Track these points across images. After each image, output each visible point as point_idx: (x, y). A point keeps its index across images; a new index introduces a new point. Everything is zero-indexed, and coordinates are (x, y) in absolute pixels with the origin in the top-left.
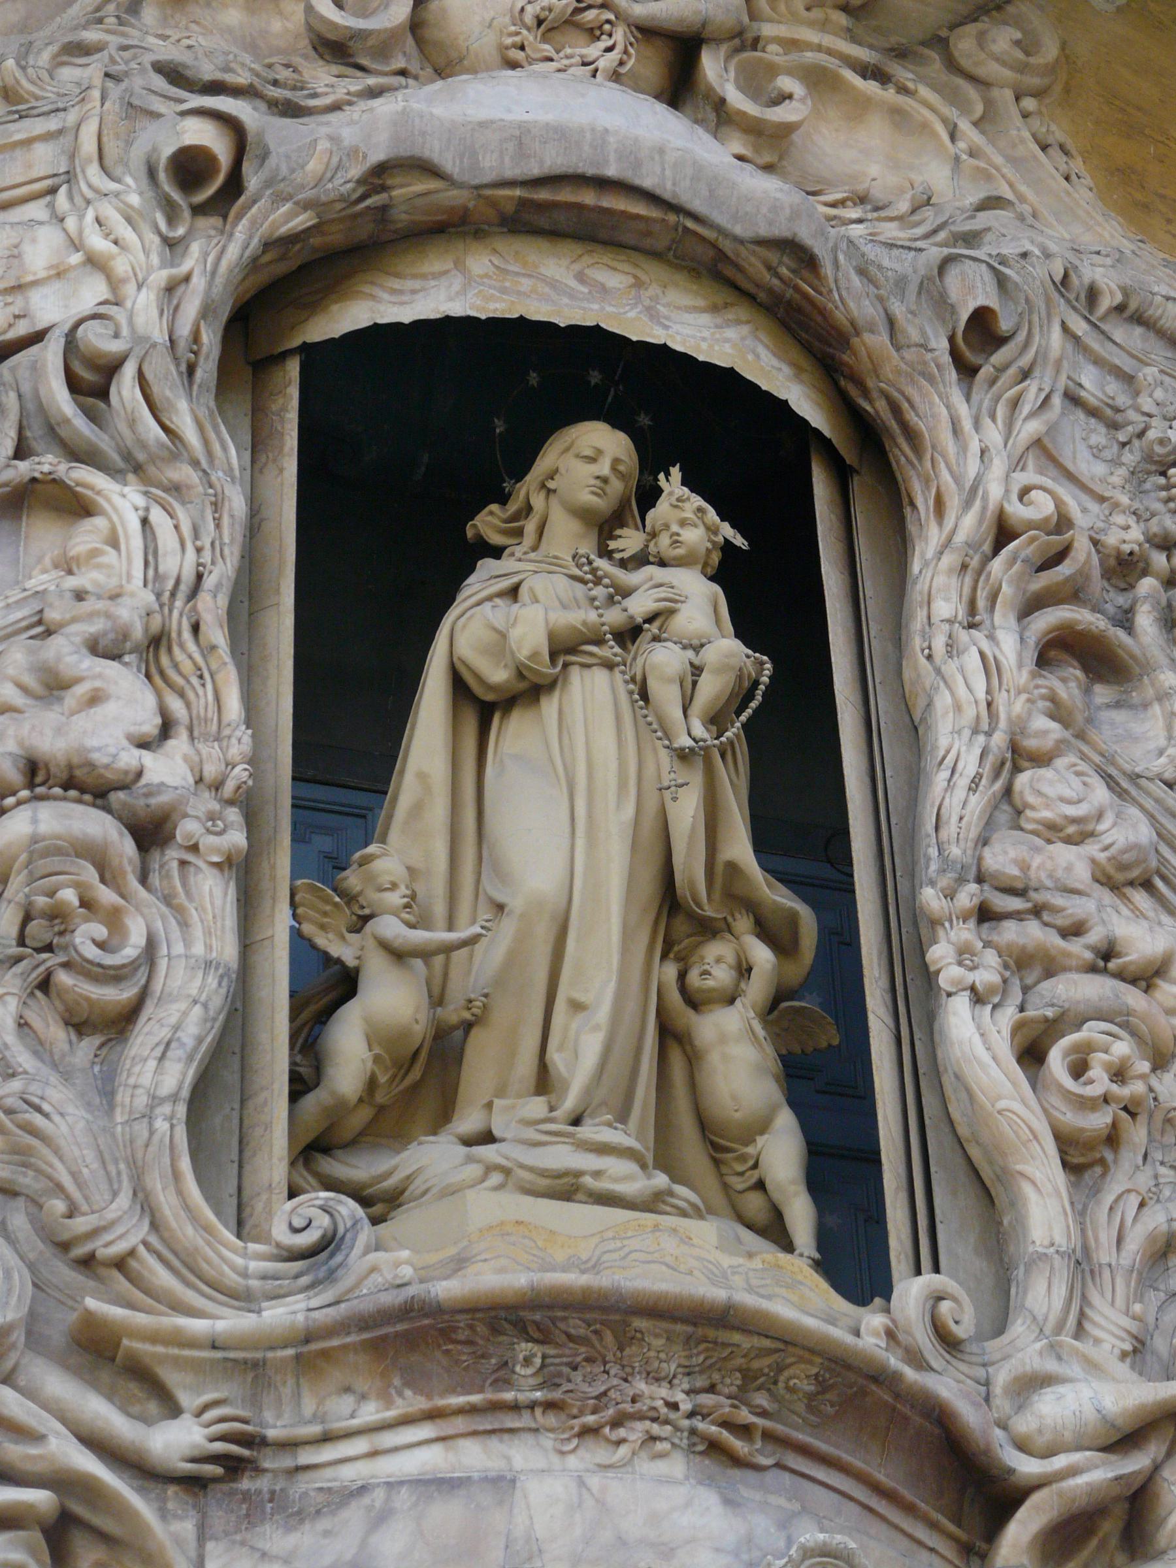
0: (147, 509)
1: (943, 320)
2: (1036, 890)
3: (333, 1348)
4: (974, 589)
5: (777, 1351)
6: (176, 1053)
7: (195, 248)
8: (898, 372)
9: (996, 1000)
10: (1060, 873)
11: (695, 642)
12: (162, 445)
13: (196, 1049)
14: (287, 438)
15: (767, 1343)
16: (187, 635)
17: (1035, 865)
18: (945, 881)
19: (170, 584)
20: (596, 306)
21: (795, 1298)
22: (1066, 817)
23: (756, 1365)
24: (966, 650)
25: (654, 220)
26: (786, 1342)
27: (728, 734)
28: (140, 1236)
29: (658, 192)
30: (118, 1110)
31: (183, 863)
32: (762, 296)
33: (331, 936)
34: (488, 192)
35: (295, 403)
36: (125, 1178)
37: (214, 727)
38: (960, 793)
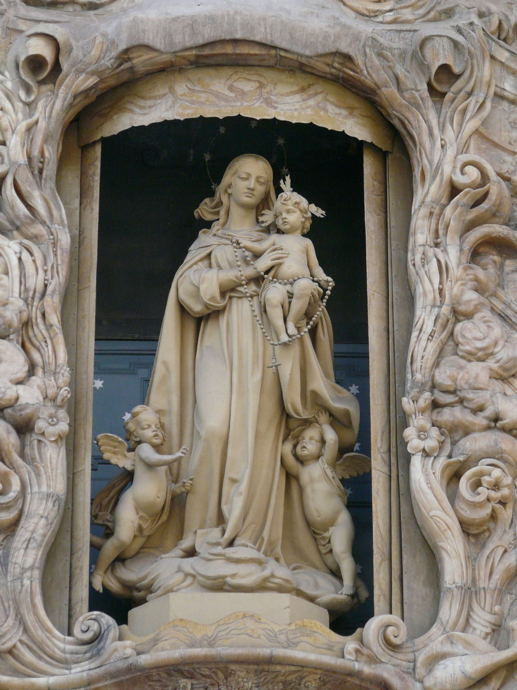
0: (20, 253)
1: (424, 73)
2: (460, 391)
3: (100, 687)
4: (437, 224)
5: (299, 671)
6: (33, 545)
7: (40, 105)
8: (401, 106)
9: (436, 454)
10: (471, 381)
11: (291, 280)
12: (27, 217)
13: (42, 541)
14: (95, 191)
15: (293, 668)
16: (40, 320)
17: (459, 378)
18: (414, 393)
19: (31, 294)
20: (238, 104)
21: (311, 640)
22: (477, 348)
23: (289, 678)
24: (431, 260)
25: (265, 55)
26: (302, 666)
27: (314, 319)
28: (18, 638)
29: (264, 41)
30: (9, 574)
31: (39, 441)
32: (328, 76)
33: (119, 457)
34: (180, 54)
35: (98, 171)
36: (12, 609)
37: (53, 367)
38: (423, 343)
